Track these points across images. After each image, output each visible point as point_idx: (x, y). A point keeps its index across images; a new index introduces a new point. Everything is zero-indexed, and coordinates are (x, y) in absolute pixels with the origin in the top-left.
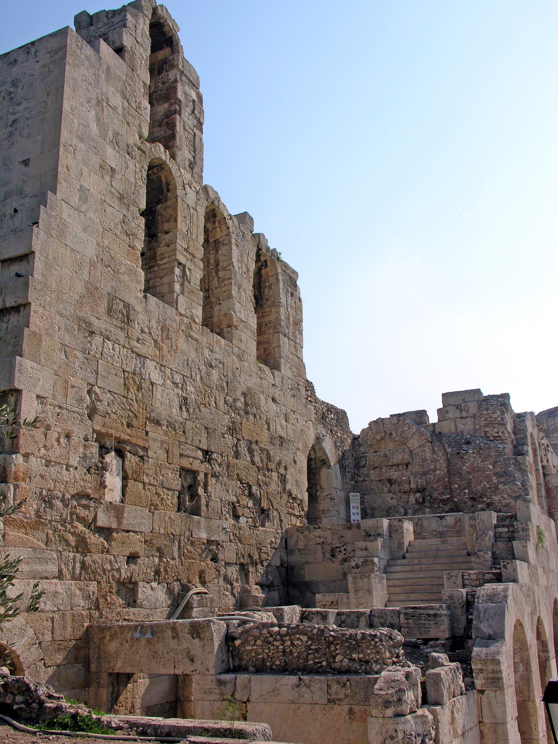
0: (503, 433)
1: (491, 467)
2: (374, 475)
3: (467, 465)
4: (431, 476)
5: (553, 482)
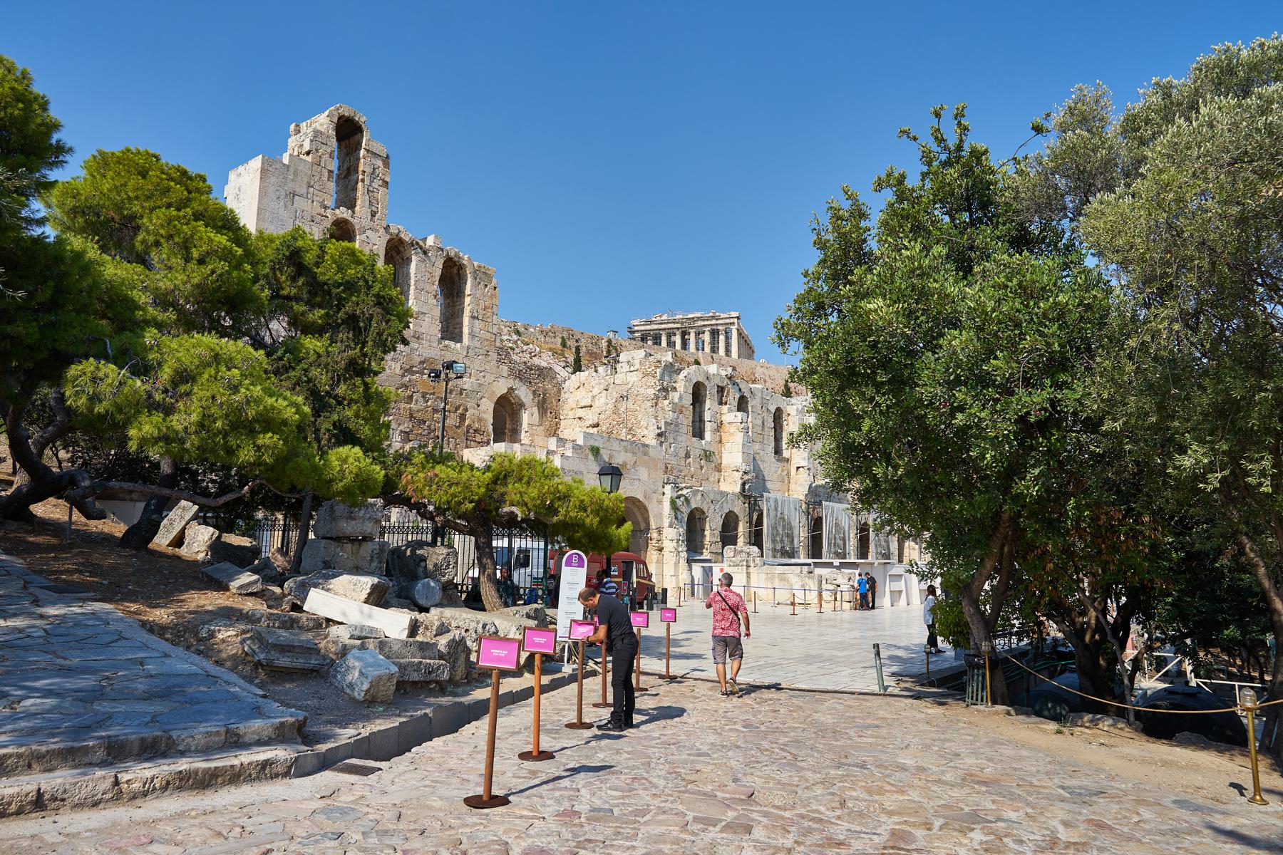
2: (571, 414)
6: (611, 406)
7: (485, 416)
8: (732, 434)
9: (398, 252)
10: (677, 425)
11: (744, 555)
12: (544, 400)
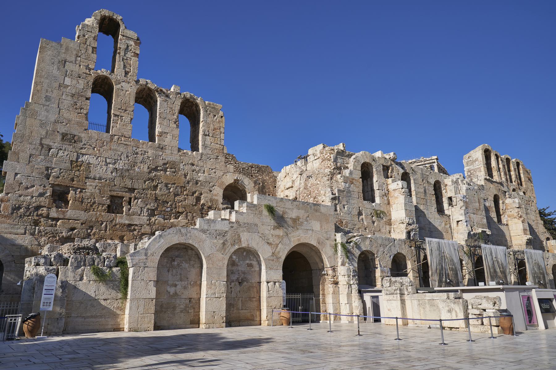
6: (303, 184)
7: (216, 198)
8: (396, 198)
9: (152, 98)
12: (263, 187)
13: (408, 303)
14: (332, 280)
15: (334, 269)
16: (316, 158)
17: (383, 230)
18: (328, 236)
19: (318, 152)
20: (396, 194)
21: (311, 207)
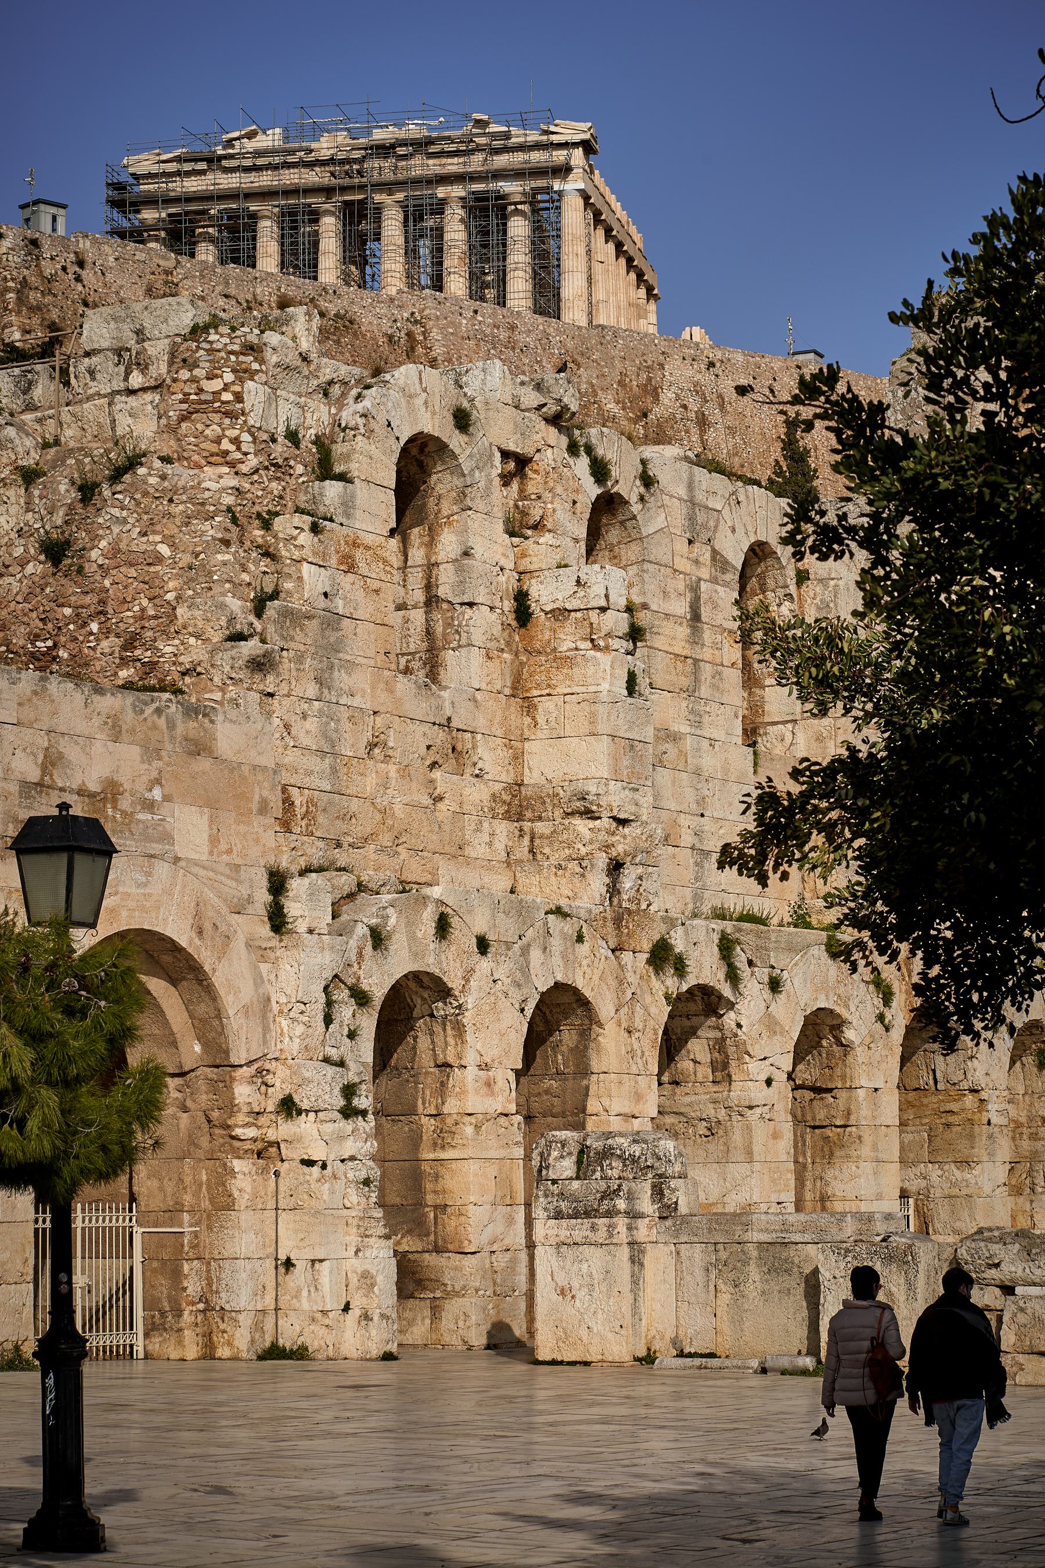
0: (236, 441)
1: (164, 550)
3: (103, 544)
4: (11, 580)
5: (543, 600)
10: (332, 620)
11: (615, 1168)
13: (659, 1260)
14: (251, 1132)
15: (260, 1072)
16: (136, 380)
17: (478, 849)
18: (245, 892)
19: (157, 349)
20: (567, 639)
21: (171, 726)
